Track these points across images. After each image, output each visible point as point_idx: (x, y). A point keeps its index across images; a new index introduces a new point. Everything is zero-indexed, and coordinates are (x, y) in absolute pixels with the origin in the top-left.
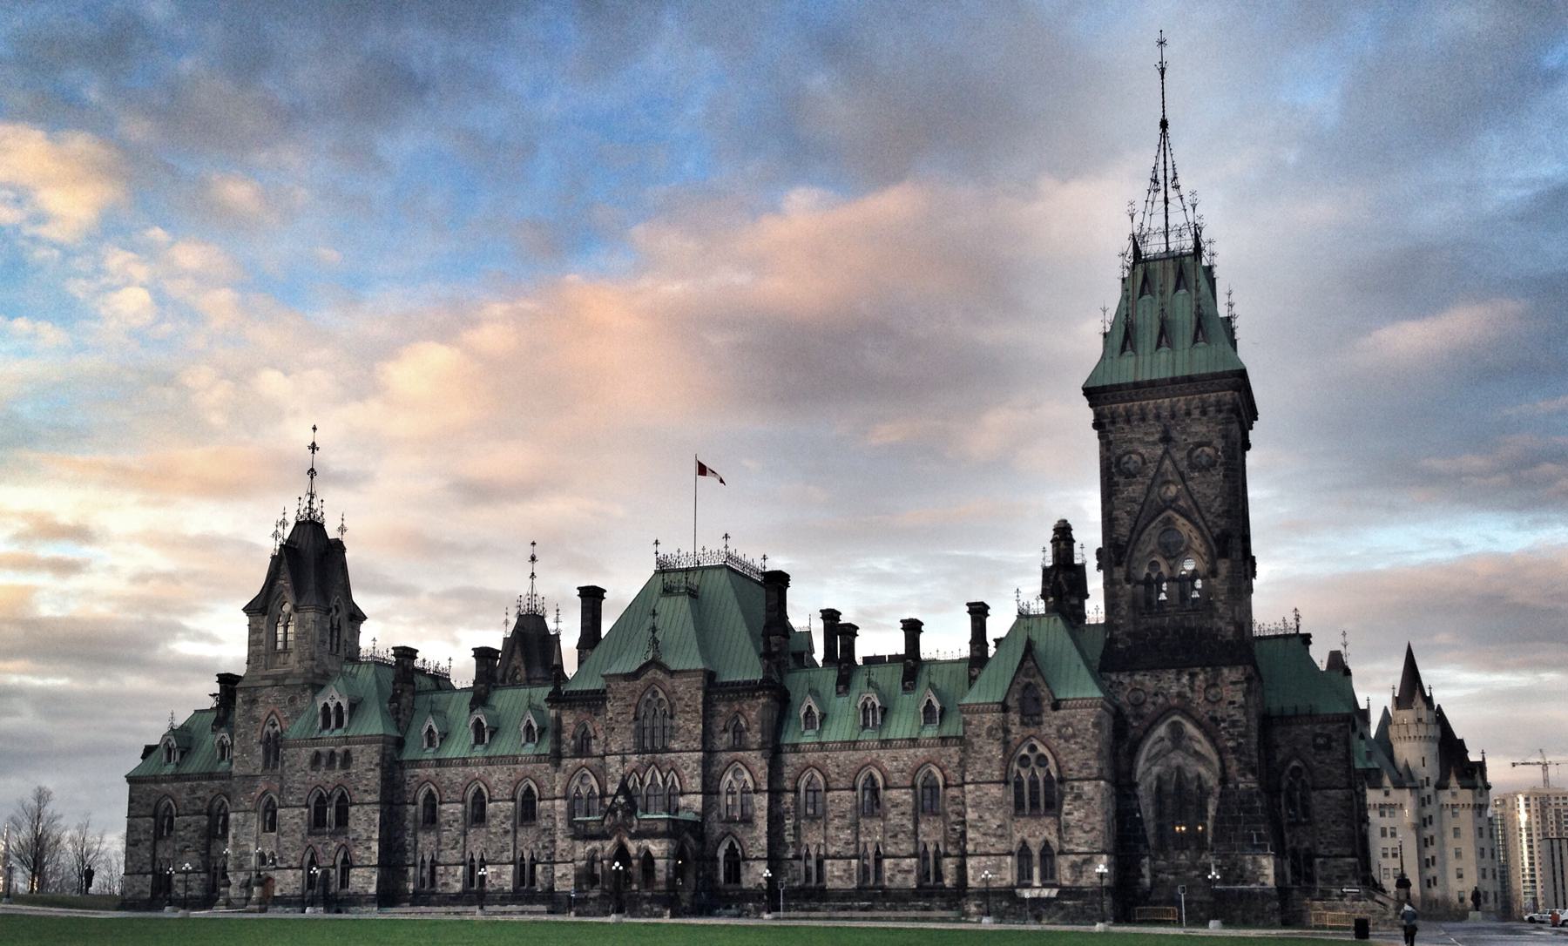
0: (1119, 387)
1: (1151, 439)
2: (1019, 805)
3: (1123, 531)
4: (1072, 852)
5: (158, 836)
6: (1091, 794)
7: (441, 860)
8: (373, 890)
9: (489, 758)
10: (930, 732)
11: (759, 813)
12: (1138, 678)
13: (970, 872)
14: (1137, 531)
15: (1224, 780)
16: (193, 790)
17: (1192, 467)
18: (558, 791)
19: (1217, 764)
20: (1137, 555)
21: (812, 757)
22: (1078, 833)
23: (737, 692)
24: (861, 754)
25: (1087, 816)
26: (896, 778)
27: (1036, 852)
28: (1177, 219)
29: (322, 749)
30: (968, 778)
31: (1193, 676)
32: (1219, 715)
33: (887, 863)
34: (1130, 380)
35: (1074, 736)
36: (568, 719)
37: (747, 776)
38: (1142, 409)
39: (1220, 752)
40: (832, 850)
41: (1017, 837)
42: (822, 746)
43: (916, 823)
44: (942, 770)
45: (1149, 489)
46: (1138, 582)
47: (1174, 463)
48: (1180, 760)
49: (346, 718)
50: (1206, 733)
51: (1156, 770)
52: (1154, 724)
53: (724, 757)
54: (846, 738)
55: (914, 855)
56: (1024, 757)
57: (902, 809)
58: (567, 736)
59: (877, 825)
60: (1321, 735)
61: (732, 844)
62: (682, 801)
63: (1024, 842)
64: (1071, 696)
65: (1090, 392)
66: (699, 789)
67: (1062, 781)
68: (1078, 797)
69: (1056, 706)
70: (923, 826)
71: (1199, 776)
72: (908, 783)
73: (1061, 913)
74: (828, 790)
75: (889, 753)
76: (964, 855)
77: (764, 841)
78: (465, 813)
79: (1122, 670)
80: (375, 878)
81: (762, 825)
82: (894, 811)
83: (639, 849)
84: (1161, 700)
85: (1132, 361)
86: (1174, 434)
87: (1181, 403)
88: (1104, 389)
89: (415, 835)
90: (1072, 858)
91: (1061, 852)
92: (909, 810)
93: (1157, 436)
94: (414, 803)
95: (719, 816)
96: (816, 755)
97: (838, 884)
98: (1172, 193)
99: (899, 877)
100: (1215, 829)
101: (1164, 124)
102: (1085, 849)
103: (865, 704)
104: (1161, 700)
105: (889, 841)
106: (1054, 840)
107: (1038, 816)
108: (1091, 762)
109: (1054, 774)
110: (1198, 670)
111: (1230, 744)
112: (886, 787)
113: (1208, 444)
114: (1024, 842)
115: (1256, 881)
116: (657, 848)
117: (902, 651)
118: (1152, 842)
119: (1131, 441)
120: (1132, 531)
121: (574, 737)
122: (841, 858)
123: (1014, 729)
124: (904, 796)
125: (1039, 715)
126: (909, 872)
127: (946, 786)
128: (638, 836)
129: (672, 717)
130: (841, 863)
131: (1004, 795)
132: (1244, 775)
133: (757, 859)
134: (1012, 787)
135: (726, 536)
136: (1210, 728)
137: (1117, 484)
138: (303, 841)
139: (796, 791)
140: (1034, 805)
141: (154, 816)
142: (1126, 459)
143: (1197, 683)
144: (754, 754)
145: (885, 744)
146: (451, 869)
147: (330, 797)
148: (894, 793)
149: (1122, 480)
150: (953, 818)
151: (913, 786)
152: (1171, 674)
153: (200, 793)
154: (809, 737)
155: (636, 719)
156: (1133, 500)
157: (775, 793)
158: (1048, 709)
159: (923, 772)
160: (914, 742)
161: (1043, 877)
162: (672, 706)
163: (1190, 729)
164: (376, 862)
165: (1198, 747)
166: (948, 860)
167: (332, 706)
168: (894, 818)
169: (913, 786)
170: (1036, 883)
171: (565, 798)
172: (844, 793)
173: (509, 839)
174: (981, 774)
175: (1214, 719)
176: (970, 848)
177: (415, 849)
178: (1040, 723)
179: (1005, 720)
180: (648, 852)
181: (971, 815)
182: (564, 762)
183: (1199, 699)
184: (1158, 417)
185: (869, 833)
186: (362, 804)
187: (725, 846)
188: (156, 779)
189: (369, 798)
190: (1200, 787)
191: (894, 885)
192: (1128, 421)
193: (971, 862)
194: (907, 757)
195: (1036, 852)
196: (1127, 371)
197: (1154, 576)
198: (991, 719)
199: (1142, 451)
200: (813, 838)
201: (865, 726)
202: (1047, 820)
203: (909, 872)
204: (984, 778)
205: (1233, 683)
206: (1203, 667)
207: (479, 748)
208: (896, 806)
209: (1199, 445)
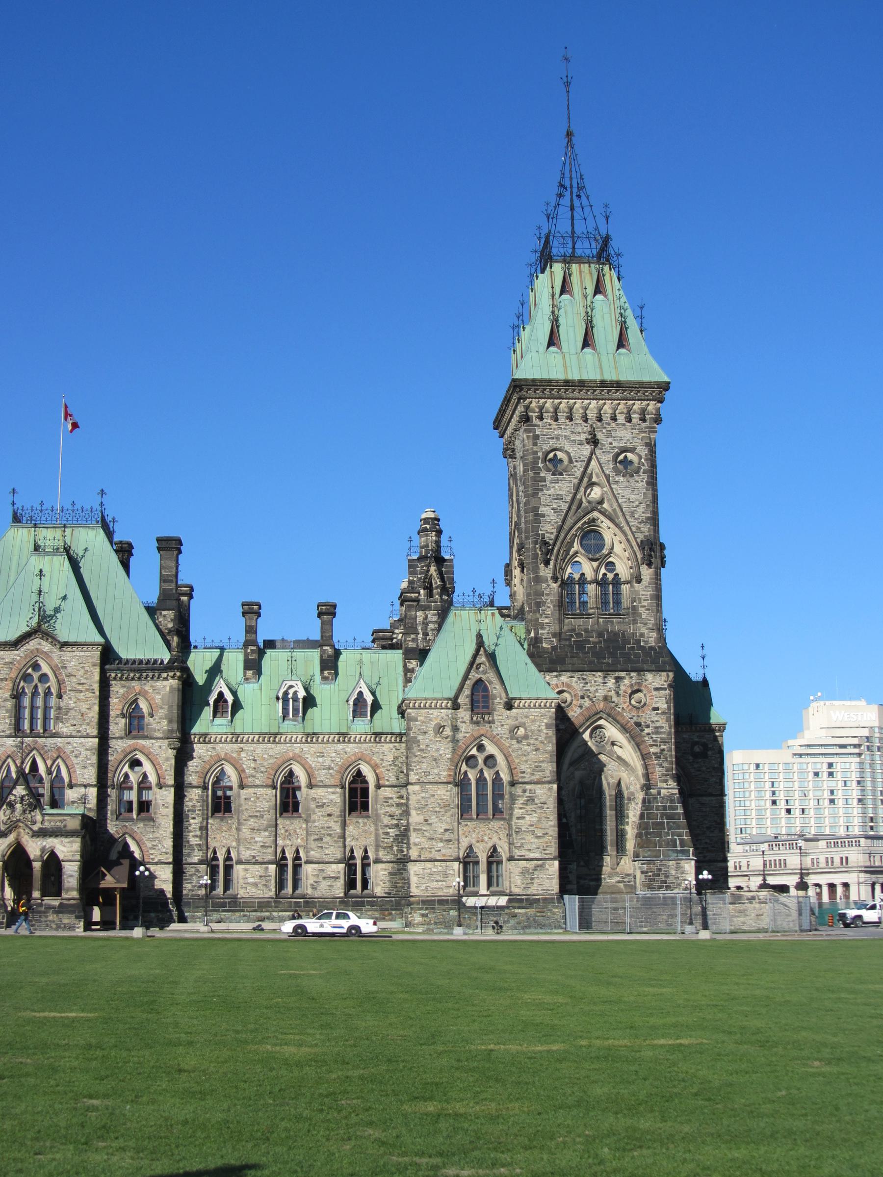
0: (549, 382)
1: (578, 438)
2: (464, 809)
4: (522, 859)
6: (543, 799)
10: (361, 726)
11: (163, 811)
13: (414, 880)
15: (647, 787)
17: (617, 471)
19: (640, 770)
21: (223, 749)
22: (529, 838)
23: (140, 671)
25: (539, 821)
26: (322, 776)
30: (413, 778)
32: (642, 721)
34: (561, 377)
39: (644, 757)
40: (246, 854)
41: (464, 843)
42: (236, 737)
43: (344, 825)
44: (375, 768)
45: (577, 488)
51: (578, 774)
54: (265, 730)
56: (473, 756)
57: (329, 810)
60: (697, 743)
63: (470, 847)
64: (523, 695)
67: (513, 784)
68: (531, 800)
69: (509, 706)
70: (350, 829)
72: (338, 782)
73: (512, 922)
74: (242, 786)
75: (315, 747)
76: (402, 862)
82: (319, 812)
83: (43, 850)
84: (587, 703)
85: (559, 357)
86: (600, 436)
91: (511, 859)
92: (336, 810)
93: (583, 437)
98: (576, 202)
100: (639, 835)
101: (569, 134)
102: (538, 855)
103: (286, 693)
104: (587, 703)
105: (313, 845)
108: (544, 765)
109: (505, 777)
110: (623, 674)
111: (653, 750)
112: (311, 786)
113: (632, 450)
114: (470, 847)
117: (317, 636)
123: (463, 727)
127: (378, 787)
130: (257, 869)
132: (666, 781)
133: (160, 863)
137: (544, 480)
140: (481, 809)
142: (551, 455)
143: (622, 687)
144: (157, 743)
145: (311, 737)
149: (549, 477)
150: (386, 820)
156: (559, 498)
158: (500, 708)
160: (343, 736)
161: (489, 884)
166: (380, 866)
168: (319, 820)
170: (483, 889)
175: (638, 724)
176: (414, 853)
178: (493, 722)
180: (53, 855)
181: (415, 818)
183: (622, 704)
185: (289, 836)
193: (414, 869)
195: (483, 858)
197: (610, 576)
199: (570, 450)
200: (222, 837)
202: (496, 824)
203: (337, 878)
204: (430, 778)
205: (656, 689)
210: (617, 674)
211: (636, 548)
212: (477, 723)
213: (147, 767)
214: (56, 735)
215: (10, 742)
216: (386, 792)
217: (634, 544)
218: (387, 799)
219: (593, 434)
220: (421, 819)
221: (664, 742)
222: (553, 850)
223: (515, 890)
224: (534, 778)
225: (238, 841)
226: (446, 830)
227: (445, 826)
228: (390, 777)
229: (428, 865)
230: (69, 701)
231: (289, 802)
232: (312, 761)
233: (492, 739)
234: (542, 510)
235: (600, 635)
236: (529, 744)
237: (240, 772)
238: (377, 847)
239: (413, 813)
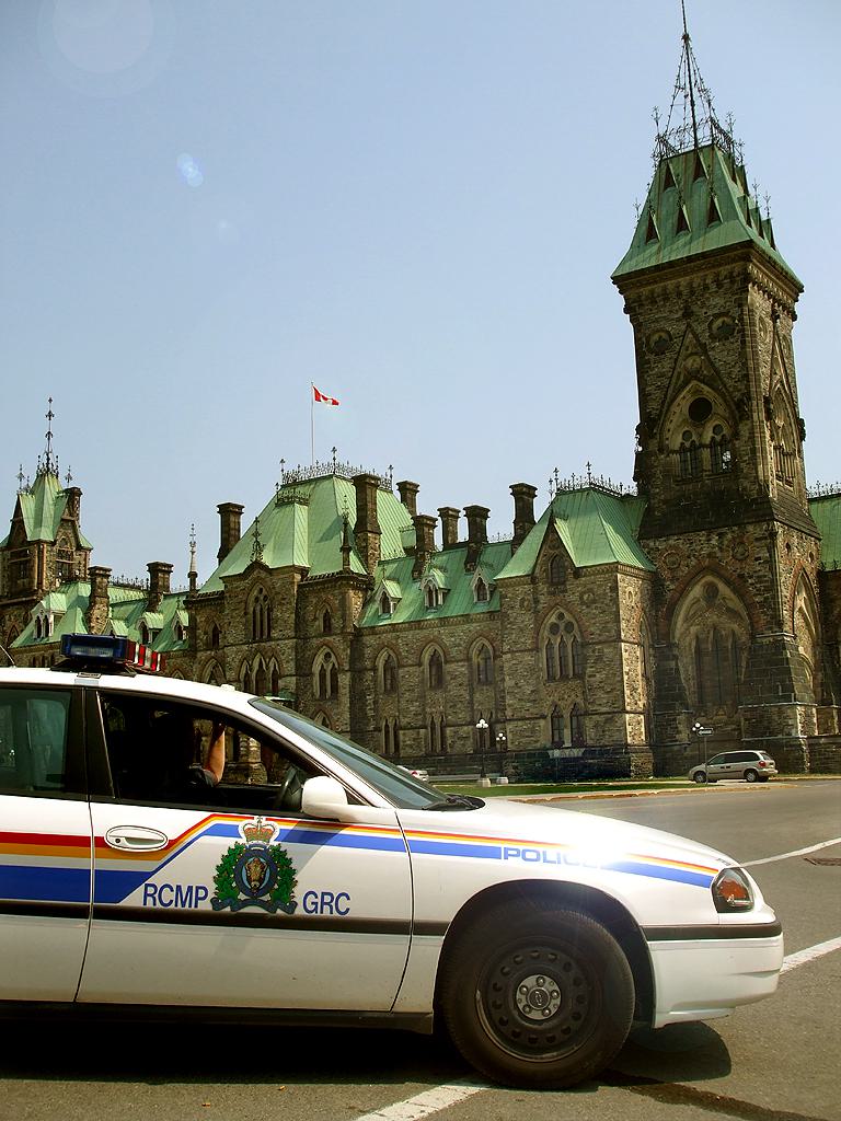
3: (653, 406)
12: (671, 542)
15: (753, 637)
17: (712, 337)
20: (669, 425)
22: (600, 694)
24: (426, 632)
25: (607, 678)
26: (454, 652)
28: (702, 112)
29: (37, 654)
33: (448, 731)
35: (594, 601)
39: (749, 606)
40: (404, 721)
46: (674, 452)
47: (696, 336)
49: (52, 628)
50: (735, 591)
51: (693, 629)
59: (439, 695)
65: (616, 280)
66: (293, 672)
67: (584, 645)
71: (733, 632)
79: (658, 537)
81: (345, 700)
84: (693, 562)
86: (695, 309)
87: (697, 279)
88: (629, 275)
92: (465, 680)
93: (680, 313)
95: (313, 695)
101: (686, 38)
112: (447, 662)
113: (726, 314)
115: (782, 731)
118: (691, 699)
119: (657, 321)
121: (206, 633)
122: (412, 728)
123: (542, 599)
125: (564, 583)
132: (771, 628)
136: (738, 585)
139: (375, 669)
152: (702, 536)
155: (246, 614)
156: (662, 375)
157: (357, 672)
163: (721, 586)
165: (731, 605)
169: (468, 659)
175: (741, 576)
179: (535, 592)
182: (199, 655)
184: (679, 294)
185: (434, 705)
191: (455, 751)
192: (653, 302)
195: (567, 715)
196: (650, 259)
205: (757, 539)
209: (717, 316)
210: (720, 530)
211: (734, 407)
212: (553, 594)
215: (245, 647)
217: (732, 403)
219: (686, 308)
221: (767, 590)
226: (532, 691)
227: (531, 688)
229: (520, 723)
232: (448, 641)
236: (596, 608)
237: (398, 654)
239: (507, 678)
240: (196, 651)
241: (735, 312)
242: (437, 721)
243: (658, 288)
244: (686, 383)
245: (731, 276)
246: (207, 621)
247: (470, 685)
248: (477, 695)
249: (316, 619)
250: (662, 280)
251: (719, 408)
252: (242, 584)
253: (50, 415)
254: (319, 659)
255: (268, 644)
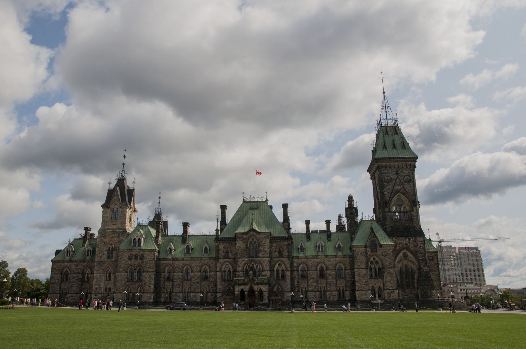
0: (384, 158)
4: (387, 289)
5: (62, 281)
7: (174, 291)
8: (151, 301)
9: (192, 258)
13: (357, 296)
14: (391, 198)
15: (419, 269)
16: (77, 266)
18: (218, 269)
19: (417, 264)
20: (391, 205)
22: (389, 283)
23: (280, 239)
24: (317, 260)
26: (330, 267)
27: (377, 289)
30: (356, 267)
31: (409, 239)
34: (388, 156)
35: (386, 255)
36: (221, 246)
37: (283, 266)
38: (390, 165)
39: (418, 260)
42: (306, 257)
43: (336, 281)
44: (344, 265)
45: (394, 186)
48: (406, 263)
51: (400, 266)
52: (399, 252)
53: (275, 260)
54: (314, 255)
55: (336, 291)
56: (372, 261)
57: (332, 276)
58: (221, 252)
59: (324, 281)
61: (278, 287)
62: (263, 273)
66: (269, 269)
67: (383, 268)
68: (389, 273)
73: (386, 307)
74: (308, 270)
75: (328, 259)
76: (353, 291)
77: (289, 286)
78: (182, 276)
80: (152, 297)
81: (289, 281)
85: (386, 152)
86: (399, 172)
87: (400, 164)
89: (164, 283)
90: (388, 291)
92: (334, 277)
93: (395, 173)
94: (164, 272)
96: (304, 260)
97: (312, 299)
99: (332, 297)
101: (384, 93)
104: (401, 245)
105: (328, 286)
106: (382, 285)
107: (377, 278)
112: (327, 270)
113: (409, 176)
116: (265, 288)
119: (387, 173)
120: (390, 198)
121: (223, 252)
122: (313, 291)
123: (369, 253)
124: (333, 273)
125: (376, 248)
126: (335, 295)
127: (345, 270)
128: (258, 284)
129: (259, 247)
130: (314, 293)
131: (367, 273)
133: (287, 292)
134: (368, 270)
135: (266, 193)
136: (414, 254)
138: (125, 284)
139: (298, 271)
141: (61, 274)
144: (285, 259)
146: (178, 294)
147: (135, 269)
148: (329, 272)
149: (386, 184)
150: (348, 279)
151: (335, 270)
153: (79, 267)
154: (301, 254)
156: (389, 189)
157: (292, 271)
158: (379, 247)
159: (338, 265)
161: (379, 297)
162: (259, 243)
164: (153, 291)
165: (411, 259)
166: (347, 292)
167: (137, 239)
168: (330, 279)
169: (335, 270)
171: (221, 271)
172: (313, 272)
173: (199, 285)
174: (359, 266)
175: (416, 251)
176: (357, 288)
177: (164, 288)
181: (357, 278)
182: (220, 260)
183: (411, 246)
184: (394, 167)
186: (148, 272)
187: (276, 287)
188: (63, 261)
189: (150, 270)
190: (412, 270)
191: (330, 300)
192: (386, 167)
193: (357, 293)
194: (333, 261)
195: (377, 289)
198: (362, 250)
201: (319, 251)
202: (379, 280)
203: (335, 295)
204: (361, 267)
206: (412, 236)
207: (187, 255)
208: (330, 275)
209: (406, 176)
213: (283, 266)
214: (260, 257)
215: (246, 259)
216: (348, 271)
218: (348, 273)
220: (358, 279)
221: (423, 256)
222: (396, 287)
223: (386, 298)
224: (390, 266)
225: (308, 285)
228: (349, 267)
230: (261, 248)
231: (322, 275)
233: (377, 256)
234: (385, 193)
235: (403, 226)
237: (308, 266)
238: (346, 286)
240: (219, 258)
241: (411, 175)
242: (323, 289)
243: (388, 164)
244: (397, 193)
245: (410, 165)
246: (224, 248)
247: (336, 278)
248: (338, 281)
249: (276, 251)
250: (390, 162)
251: (407, 201)
252: (245, 236)
253: (125, 156)
254: (277, 266)
255: (257, 259)
